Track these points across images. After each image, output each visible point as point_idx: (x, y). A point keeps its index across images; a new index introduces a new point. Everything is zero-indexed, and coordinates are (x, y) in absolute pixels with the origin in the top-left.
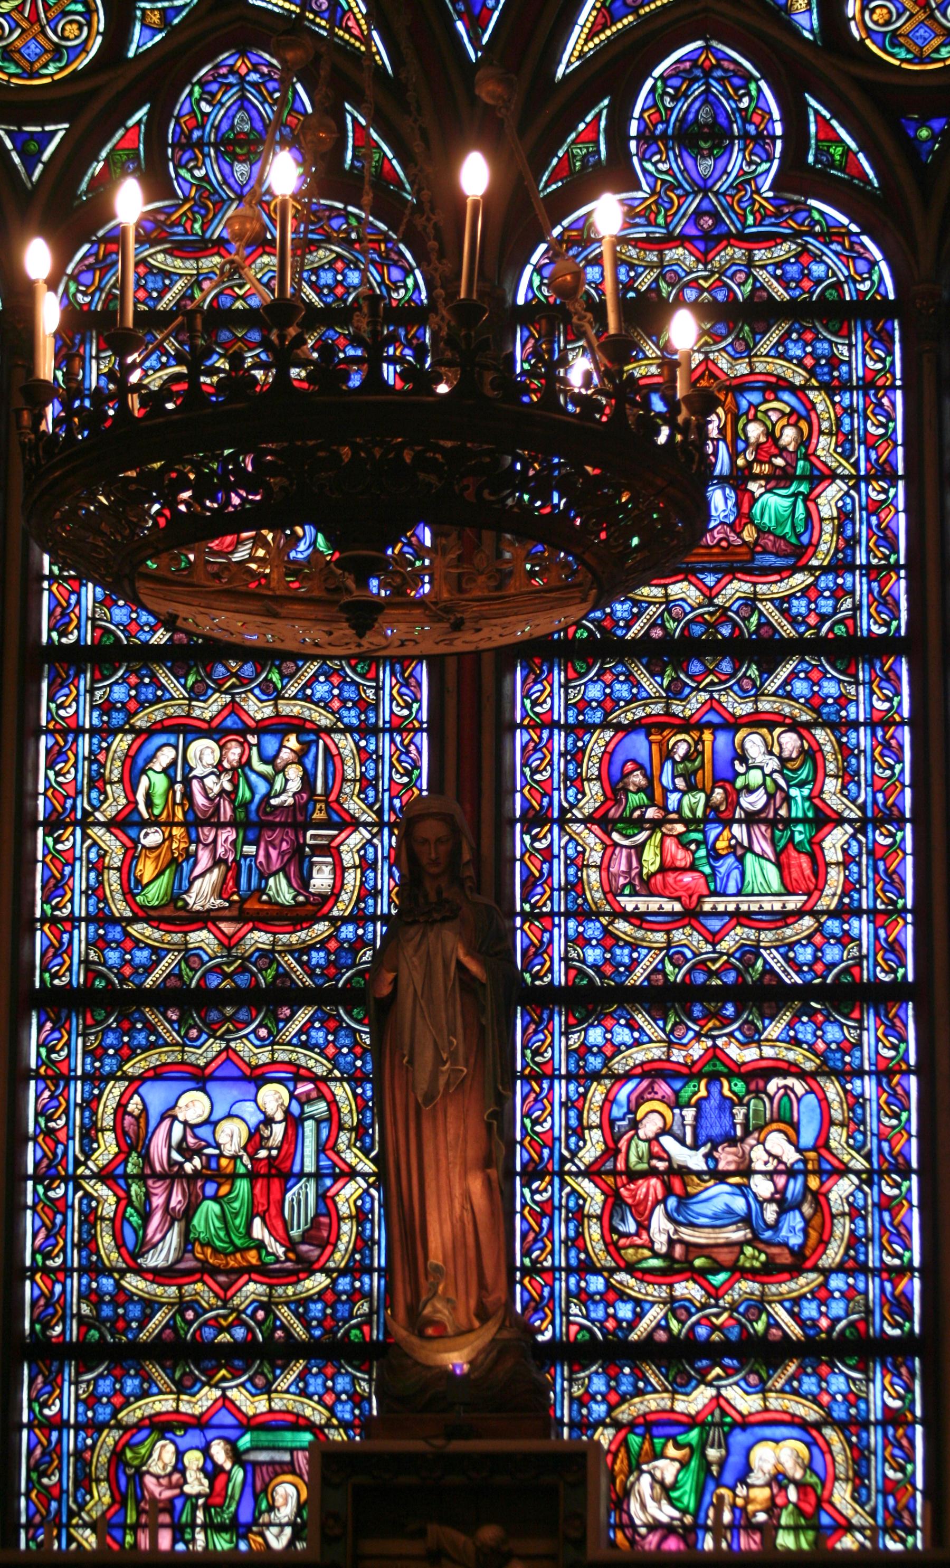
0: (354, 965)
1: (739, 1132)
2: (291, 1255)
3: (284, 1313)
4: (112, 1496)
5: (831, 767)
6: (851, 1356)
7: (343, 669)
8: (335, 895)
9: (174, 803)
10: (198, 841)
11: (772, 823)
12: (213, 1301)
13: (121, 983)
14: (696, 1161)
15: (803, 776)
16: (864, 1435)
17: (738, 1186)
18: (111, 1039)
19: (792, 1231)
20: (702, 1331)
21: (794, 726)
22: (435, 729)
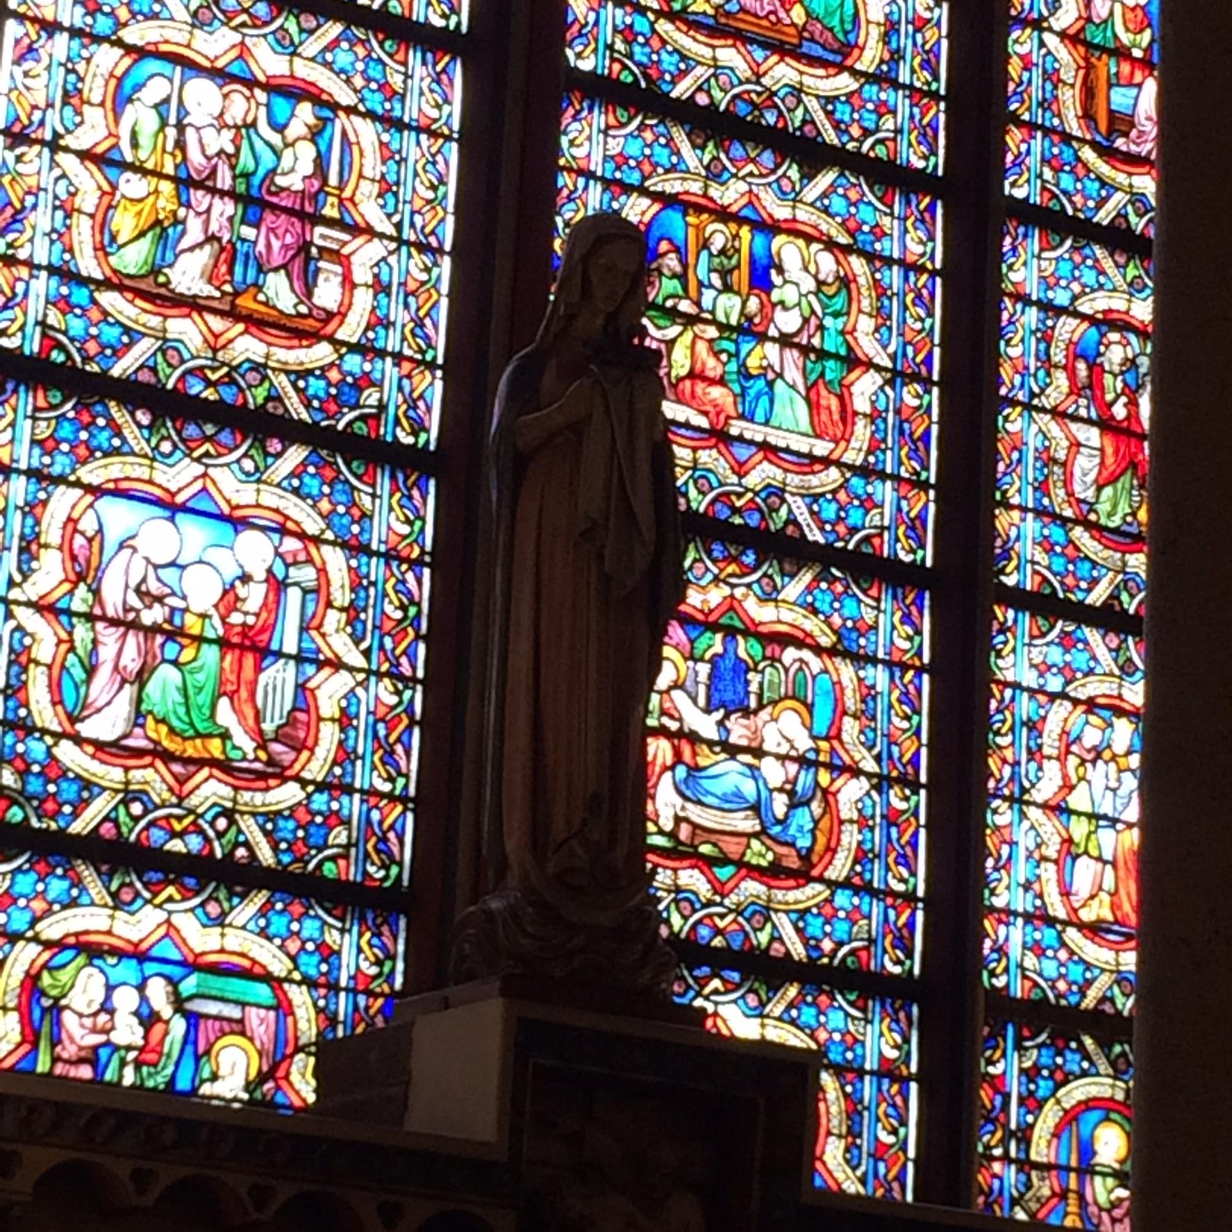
0: (356, 406)
1: (753, 703)
2: (263, 755)
3: (250, 828)
4: (22, 1033)
5: (865, 304)
6: (851, 990)
7: (368, 41)
8: (342, 314)
9: (164, 151)
10: (188, 206)
11: (806, 350)
12: (166, 795)
13: (84, 363)
14: (706, 726)
15: (838, 307)
16: (859, 1086)
17: (750, 766)
18: (66, 431)
20: (704, 932)
21: (830, 245)
22: (467, 139)
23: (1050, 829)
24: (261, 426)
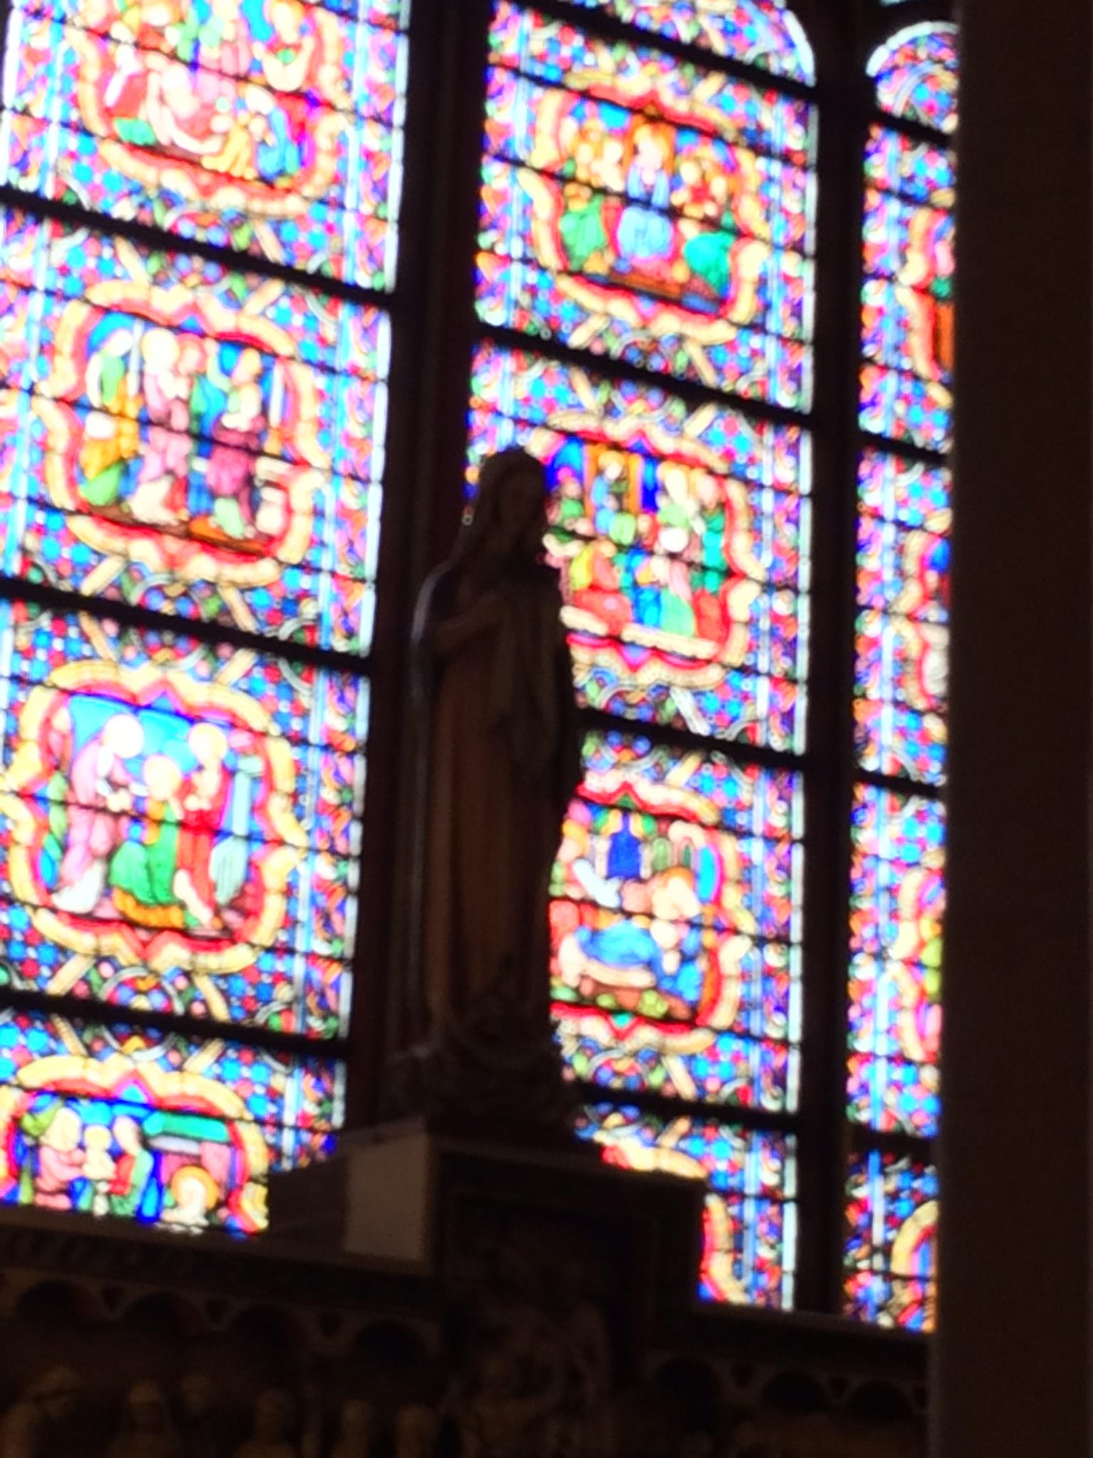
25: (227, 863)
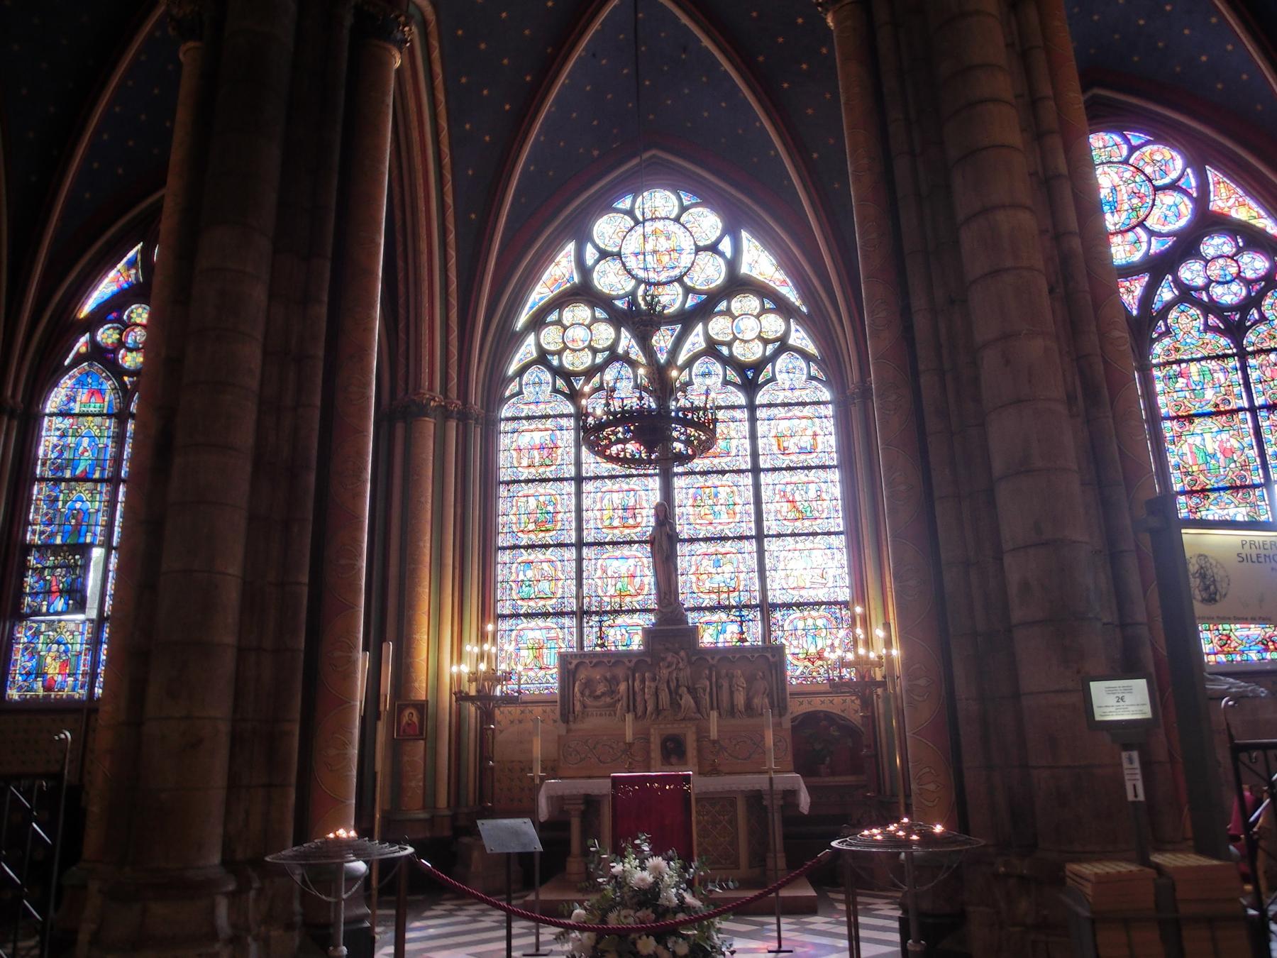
14: (713, 571)
19: (733, 584)
23: (783, 574)
24: (630, 543)
25: (637, 580)
